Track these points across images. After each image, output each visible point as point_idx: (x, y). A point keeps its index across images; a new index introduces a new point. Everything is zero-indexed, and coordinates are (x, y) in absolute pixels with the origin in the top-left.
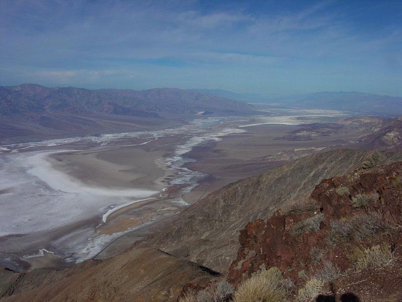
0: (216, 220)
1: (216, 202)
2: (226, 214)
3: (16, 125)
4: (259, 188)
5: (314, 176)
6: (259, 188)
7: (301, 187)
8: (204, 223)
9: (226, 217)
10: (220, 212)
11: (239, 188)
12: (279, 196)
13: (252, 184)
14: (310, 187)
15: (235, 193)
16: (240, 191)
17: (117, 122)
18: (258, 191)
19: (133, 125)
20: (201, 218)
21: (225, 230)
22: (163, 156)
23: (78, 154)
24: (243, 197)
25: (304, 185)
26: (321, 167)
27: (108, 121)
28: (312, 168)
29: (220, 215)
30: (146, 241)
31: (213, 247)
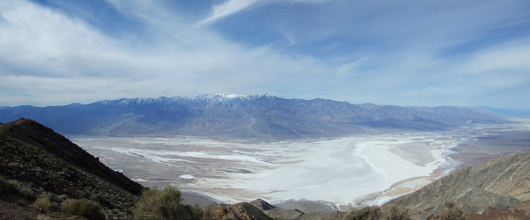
1: (436, 183)
4: (468, 176)
5: (509, 171)
6: (468, 176)
7: (498, 178)
9: (442, 194)
10: (438, 190)
11: (454, 175)
12: (480, 184)
13: (464, 173)
14: (505, 179)
15: (451, 178)
16: (455, 177)
18: (467, 178)
24: (456, 181)
25: (500, 176)
26: (515, 164)
28: (508, 165)
29: (438, 192)
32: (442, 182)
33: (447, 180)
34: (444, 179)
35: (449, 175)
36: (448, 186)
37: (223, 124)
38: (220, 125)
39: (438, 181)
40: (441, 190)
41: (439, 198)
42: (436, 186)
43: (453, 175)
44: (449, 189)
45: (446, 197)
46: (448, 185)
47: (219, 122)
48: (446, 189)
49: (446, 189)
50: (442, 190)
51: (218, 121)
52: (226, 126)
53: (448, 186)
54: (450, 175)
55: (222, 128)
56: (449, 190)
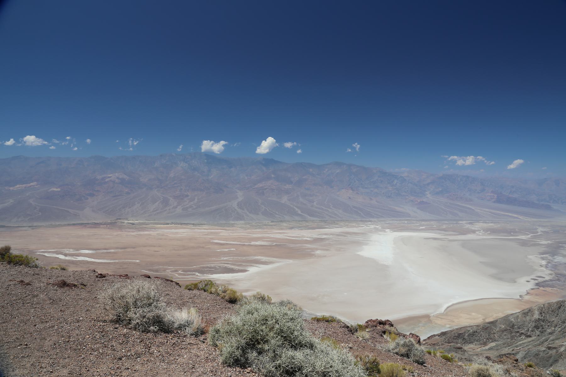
0: (522, 333)
2: (539, 330)
3: (396, 208)
8: (505, 333)
9: (538, 333)
15: (560, 308)
17: (498, 212)
19: (516, 216)
20: (503, 326)
21: (509, 346)
22: (539, 253)
23: (444, 240)
27: (487, 210)
29: (530, 329)
30: (439, 336)
31: (463, 357)
32: (541, 313)
33: (551, 309)
34: (544, 308)
35: (556, 302)
36: (552, 320)
37: (196, 200)
38: (192, 203)
39: (531, 310)
40: (537, 327)
41: (530, 339)
42: (528, 318)
43: (562, 301)
44: (555, 327)
45: (545, 339)
46: (553, 319)
47: (189, 197)
48: (548, 326)
49: (548, 326)
50: (539, 325)
51: (187, 196)
52: (200, 203)
53: (553, 321)
54: (558, 303)
55: (195, 207)
56: (553, 329)
